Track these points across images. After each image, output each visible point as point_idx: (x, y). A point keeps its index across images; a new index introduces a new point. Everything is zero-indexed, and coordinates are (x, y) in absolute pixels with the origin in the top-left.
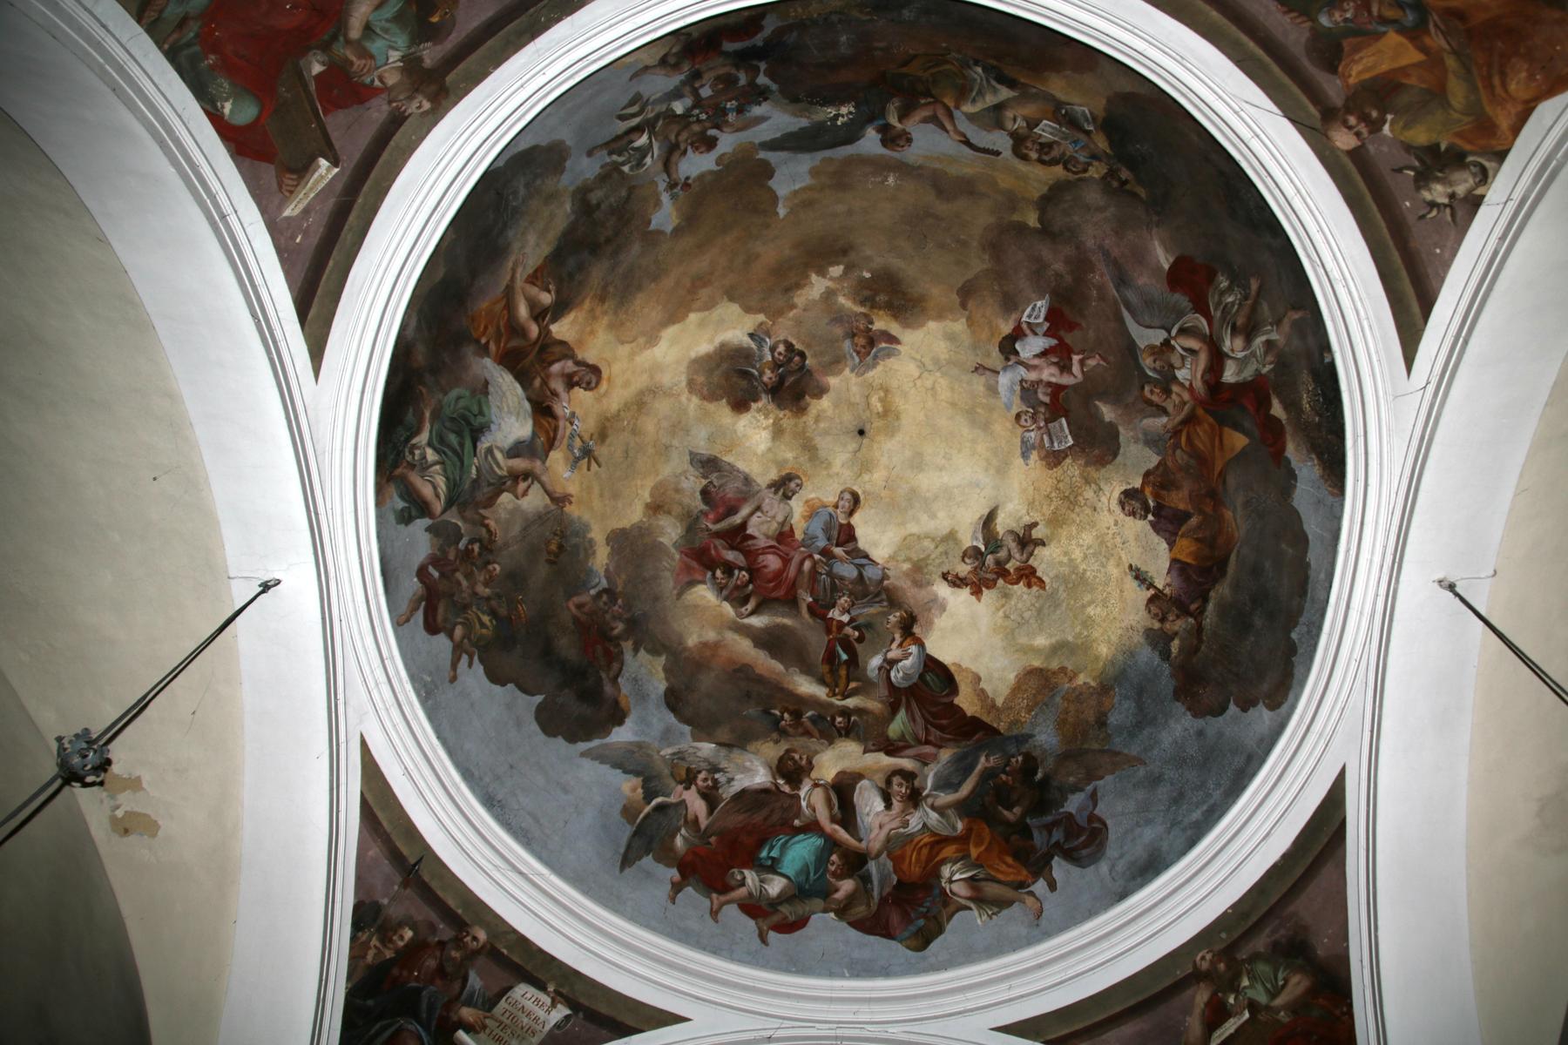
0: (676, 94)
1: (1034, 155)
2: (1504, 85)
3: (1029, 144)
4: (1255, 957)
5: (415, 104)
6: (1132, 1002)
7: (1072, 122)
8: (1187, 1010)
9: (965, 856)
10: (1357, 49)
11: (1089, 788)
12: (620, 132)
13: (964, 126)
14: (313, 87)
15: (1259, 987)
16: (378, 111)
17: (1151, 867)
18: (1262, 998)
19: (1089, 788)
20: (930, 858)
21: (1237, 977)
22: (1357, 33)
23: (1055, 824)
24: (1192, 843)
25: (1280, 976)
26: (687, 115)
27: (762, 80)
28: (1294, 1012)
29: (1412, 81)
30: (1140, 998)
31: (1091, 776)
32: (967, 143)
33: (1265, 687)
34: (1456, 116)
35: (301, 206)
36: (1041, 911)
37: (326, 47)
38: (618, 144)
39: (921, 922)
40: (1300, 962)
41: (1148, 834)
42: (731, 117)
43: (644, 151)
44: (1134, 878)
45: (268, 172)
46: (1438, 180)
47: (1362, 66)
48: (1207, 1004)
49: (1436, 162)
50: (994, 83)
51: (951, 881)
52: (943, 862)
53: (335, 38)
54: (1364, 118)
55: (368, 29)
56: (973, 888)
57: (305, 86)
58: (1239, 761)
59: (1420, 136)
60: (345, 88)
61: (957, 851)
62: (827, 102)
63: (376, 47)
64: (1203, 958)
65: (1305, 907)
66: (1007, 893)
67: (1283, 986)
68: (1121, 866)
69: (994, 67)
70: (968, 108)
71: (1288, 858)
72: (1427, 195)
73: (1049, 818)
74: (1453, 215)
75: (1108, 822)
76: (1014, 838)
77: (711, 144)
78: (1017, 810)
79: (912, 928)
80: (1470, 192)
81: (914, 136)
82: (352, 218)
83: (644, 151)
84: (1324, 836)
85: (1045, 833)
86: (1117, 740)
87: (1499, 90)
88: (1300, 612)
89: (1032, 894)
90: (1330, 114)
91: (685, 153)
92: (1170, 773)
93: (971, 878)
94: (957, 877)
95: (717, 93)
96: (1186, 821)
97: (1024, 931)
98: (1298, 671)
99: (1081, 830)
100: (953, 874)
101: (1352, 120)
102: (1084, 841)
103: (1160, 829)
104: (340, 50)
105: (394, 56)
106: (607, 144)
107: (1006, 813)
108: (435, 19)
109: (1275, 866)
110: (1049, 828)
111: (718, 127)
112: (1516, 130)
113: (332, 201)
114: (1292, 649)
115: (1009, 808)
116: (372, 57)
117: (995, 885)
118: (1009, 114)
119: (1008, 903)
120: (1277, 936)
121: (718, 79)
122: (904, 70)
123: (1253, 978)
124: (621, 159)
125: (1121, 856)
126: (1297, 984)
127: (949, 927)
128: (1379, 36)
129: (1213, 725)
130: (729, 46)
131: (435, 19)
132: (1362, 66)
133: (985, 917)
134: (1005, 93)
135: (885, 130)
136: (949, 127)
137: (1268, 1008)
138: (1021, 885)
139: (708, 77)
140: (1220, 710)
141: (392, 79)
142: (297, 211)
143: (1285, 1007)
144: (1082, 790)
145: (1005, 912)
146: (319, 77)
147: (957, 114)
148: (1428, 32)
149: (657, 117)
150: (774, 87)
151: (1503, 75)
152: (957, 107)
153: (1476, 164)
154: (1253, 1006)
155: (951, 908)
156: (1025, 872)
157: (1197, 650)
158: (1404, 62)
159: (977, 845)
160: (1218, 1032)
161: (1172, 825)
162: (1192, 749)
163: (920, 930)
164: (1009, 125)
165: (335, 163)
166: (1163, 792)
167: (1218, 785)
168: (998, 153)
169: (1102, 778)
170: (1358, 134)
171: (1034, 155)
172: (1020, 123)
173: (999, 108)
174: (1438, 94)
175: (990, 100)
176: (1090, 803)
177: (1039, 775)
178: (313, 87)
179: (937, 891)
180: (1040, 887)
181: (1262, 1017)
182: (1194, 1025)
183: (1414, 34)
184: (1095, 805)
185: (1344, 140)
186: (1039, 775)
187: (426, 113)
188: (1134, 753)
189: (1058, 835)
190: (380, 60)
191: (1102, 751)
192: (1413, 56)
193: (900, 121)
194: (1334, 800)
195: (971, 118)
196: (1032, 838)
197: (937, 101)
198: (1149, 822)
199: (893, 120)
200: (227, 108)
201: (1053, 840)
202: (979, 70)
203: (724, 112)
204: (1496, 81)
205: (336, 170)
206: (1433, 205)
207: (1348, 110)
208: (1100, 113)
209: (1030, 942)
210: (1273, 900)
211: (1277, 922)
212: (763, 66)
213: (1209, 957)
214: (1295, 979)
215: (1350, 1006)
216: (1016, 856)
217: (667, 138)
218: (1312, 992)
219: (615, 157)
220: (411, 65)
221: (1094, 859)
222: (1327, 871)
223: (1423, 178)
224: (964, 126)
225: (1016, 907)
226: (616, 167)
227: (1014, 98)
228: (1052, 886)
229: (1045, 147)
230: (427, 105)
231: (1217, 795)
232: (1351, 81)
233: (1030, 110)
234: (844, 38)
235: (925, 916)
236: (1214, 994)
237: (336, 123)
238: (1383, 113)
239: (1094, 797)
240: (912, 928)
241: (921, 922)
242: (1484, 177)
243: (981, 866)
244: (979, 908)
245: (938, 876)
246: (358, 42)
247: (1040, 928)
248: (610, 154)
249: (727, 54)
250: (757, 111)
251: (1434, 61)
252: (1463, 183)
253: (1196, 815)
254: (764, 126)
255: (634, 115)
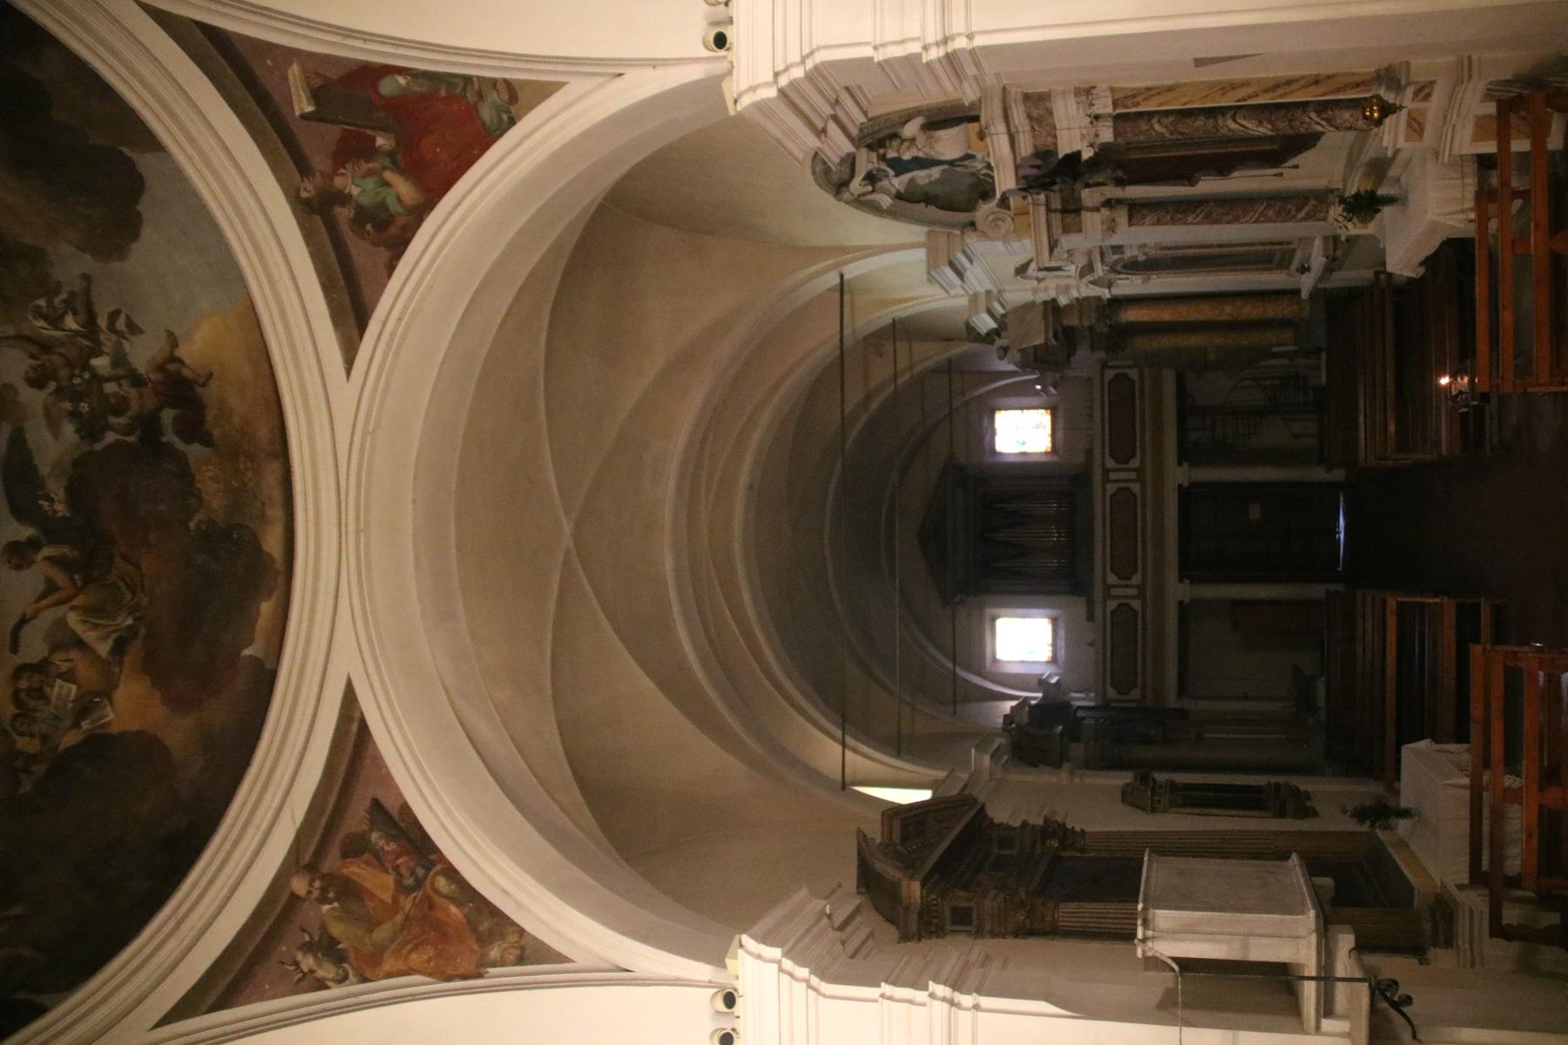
0: (119, 360)
1: (23, 684)
2: (411, 951)
3: (37, 677)
5: (310, 187)
7: (85, 708)
10: (367, 863)
12: (97, 308)
13: (48, 618)
14: (369, 132)
16: (320, 161)
22: (379, 859)
26: (86, 366)
27: (110, 437)
29: (370, 905)
32: (23, 621)
34: (367, 941)
35: (291, 78)
37: (391, 154)
38: (83, 304)
42: (68, 406)
43: (55, 321)
45: (334, 74)
46: (316, 958)
47: (359, 871)
49: (328, 948)
50: (114, 636)
53: (394, 162)
54: (324, 890)
55: (387, 184)
57: (373, 128)
59: (336, 929)
60: (353, 150)
62: (72, 492)
63: (370, 183)
69: (136, 634)
70: (73, 619)
72: (299, 956)
74: (300, 980)
77: (37, 382)
80: (324, 979)
81: (26, 574)
82: (253, 106)
83: (55, 321)
87: (404, 952)
90: (312, 868)
91: (33, 357)
95: (107, 397)
101: (317, 884)
104: (387, 162)
105: (355, 191)
106: (87, 292)
108: (369, 227)
111: (58, 391)
112: (389, 975)
113: (277, 97)
116: (364, 176)
118: (73, 654)
121: (125, 399)
122: (118, 559)
124: (57, 301)
128: (385, 871)
130: (168, 415)
131: (369, 227)
132: (359, 871)
134: (104, 649)
135: (34, 544)
136: (44, 603)
139: (133, 393)
141: (338, 182)
142: (290, 72)
146: (373, 140)
147: (64, 608)
148: (407, 896)
149: (98, 344)
150: (98, 447)
151: (416, 947)
152: (73, 608)
153: (345, 971)
158: (379, 894)
164: (58, 658)
165: (304, 116)
168: (14, 648)
170: (310, 892)
171: (23, 684)
172: (64, 667)
173: (80, 644)
174: (371, 924)
175: (90, 636)
178: (369, 132)
183: (401, 889)
185: (299, 885)
187: (298, 191)
190: (357, 181)
192: (387, 897)
193: (47, 558)
195: (61, 623)
197: (78, 591)
199: (47, 551)
200: (402, 80)
202: (129, 622)
203: (76, 397)
204: (408, 947)
205: (297, 113)
206: (296, 964)
207: (323, 877)
208: (114, 730)
212: (132, 439)
217: (63, 344)
219: (64, 296)
220: (344, 198)
223: (309, 948)
224: (48, 618)
226: (51, 294)
227: (98, 657)
229: (39, 694)
230: (304, 195)
232: (345, 871)
233: (84, 669)
234: (162, 508)
237: (333, 132)
238: (337, 899)
242: (342, 980)
246: (380, 174)
248: (72, 294)
249: (160, 409)
250: (69, 430)
251: (394, 907)
252: (327, 971)
254: (46, 433)
255: (112, 327)
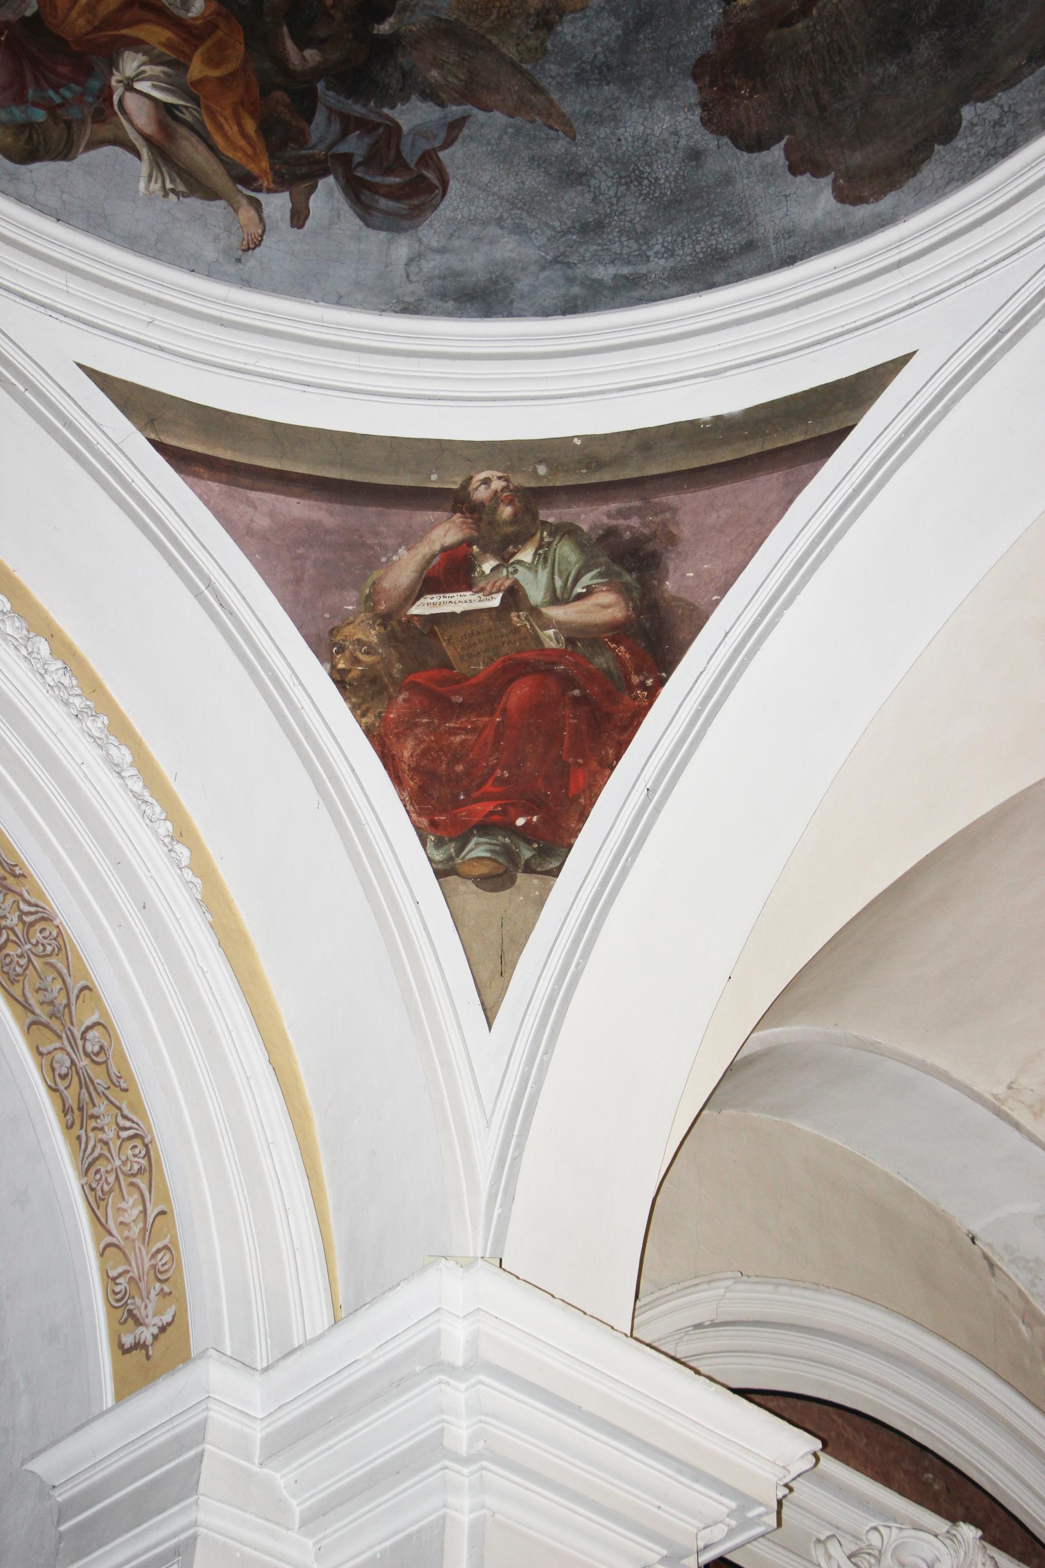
4: (567, 531)
6: (334, 474)
8: (409, 540)
9: (179, 65)
11: (455, 110)
15: (543, 575)
17: (482, 297)
18: (536, 594)
19: (455, 110)
20: (112, 21)
21: (520, 540)
23: (364, 125)
24: (570, 308)
25: (586, 580)
28: (570, 641)
30: (349, 476)
31: (471, 92)
33: (857, 158)
36: (257, 245)
39: (40, 115)
40: (628, 578)
41: (508, 248)
44: (443, 296)
48: (444, 550)
51: (129, 87)
52: (135, 44)
56: (162, 125)
58: (727, 239)
61: (169, 45)
64: (487, 481)
65: (693, 510)
66: (219, 177)
67: (580, 597)
68: (432, 265)
71: (722, 428)
73: (357, 109)
75: (454, 186)
76: (278, 95)
78: (312, 55)
79: (18, 114)
84: (801, 432)
85: (336, 127)
86: (553, 68)
88: (1010, 82)
89: (257, 205)
92: (604, 181)
93: (168, 108)
94: (144, 86)
96: (580, 271)
97: (210, 253)
98: (931, 172)
99: (399, 164)
100: (139, 77)
102: (396, 186)
103: (531, 253)
107: (290, 44)
109: (694, 424)
110: (349, 124)
114: (948, 131)
115: (302, 44)
117: (202, 148)
119: (211, 194)
120: (621, 522)
123: (543, 556)
125: (442, 251)
126: (604, 607)
127: (84, 158)
129: (724, 156)
133: (156, 186)
137: (534, 611)
138: (247, 180)
140: (758, 144)
143: (560, 626)
144: (442, 104)
145: (195, 203)
154: (514, 595)
155: (105, 131)
156: (265, 164)
157: (788, 21)
159: (210, 61)
160: (436, 598)
161: (555, 261)
162: (665, 170)
163: (30, 126)
166: (574, 201)
167: (670, 253)
169: (487, 109)
176: (443, 135)
177: (384, 28)
179: (95, 84)
180: (277, 204)
181: (516, 618)
182: (404, 567)
184: (447, 144)
186: (384, 28)
188: (566, 109)
189: (355, 145)
191: (515, 67)
194: (858, 392)
196: (309, 120)
198: (519, 230)
201: (342, 149)
209: (211, 273)
210: (653, 470)
211: (637, 503)
213: (497, 485)
214: (605, 597)
215: (661, 683)
216: (265, 128)
218: (617, 631)
221: (397, 223)
222: (768, 482)
225: (218, 207)
228: (299, 217)
231: (658, 265)
235: (52, 109)
236: (469, 542)
239: (455, 127)
240: (18, 114)
241: (40, 115)
243: (196, 100)
244: (155, 164)
245: (113, 63)
247: (240, 260)
253: (604, 273)
